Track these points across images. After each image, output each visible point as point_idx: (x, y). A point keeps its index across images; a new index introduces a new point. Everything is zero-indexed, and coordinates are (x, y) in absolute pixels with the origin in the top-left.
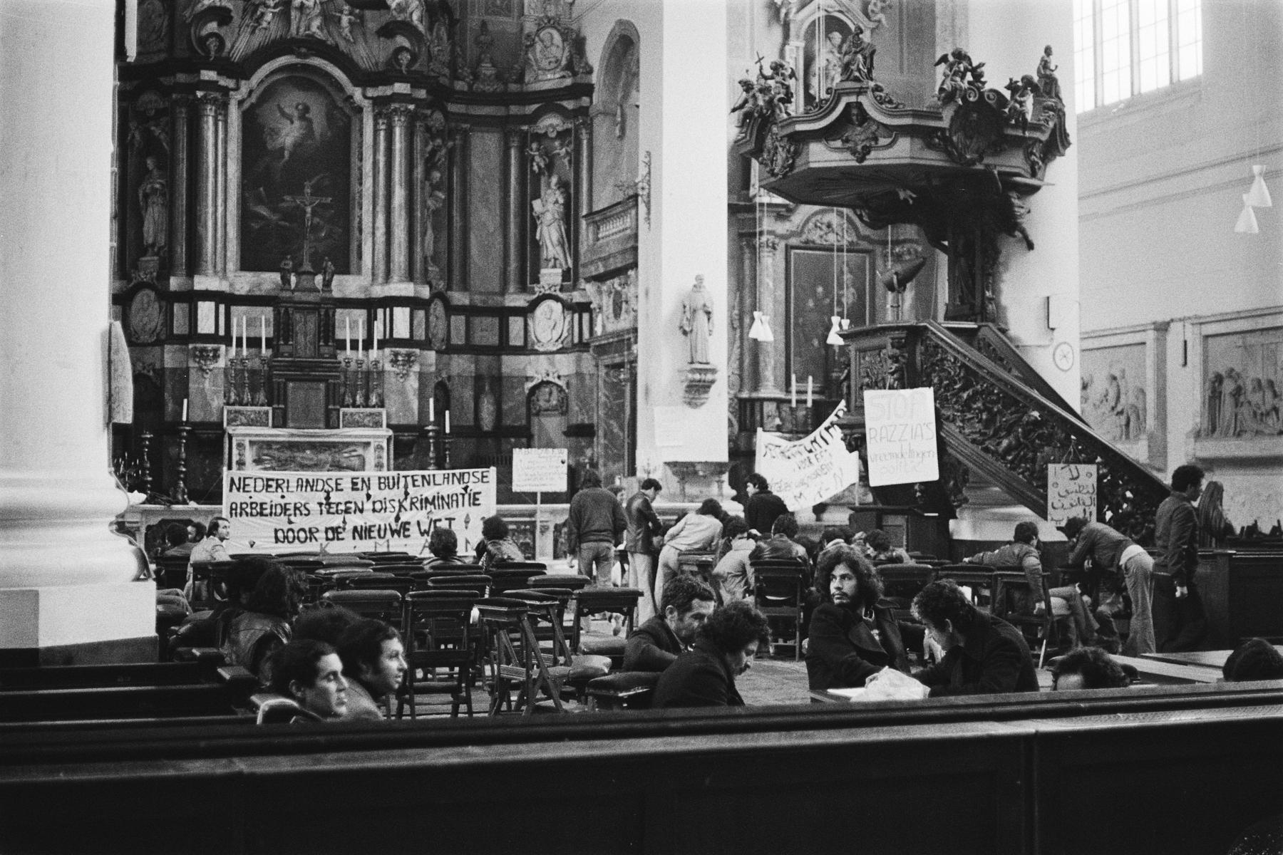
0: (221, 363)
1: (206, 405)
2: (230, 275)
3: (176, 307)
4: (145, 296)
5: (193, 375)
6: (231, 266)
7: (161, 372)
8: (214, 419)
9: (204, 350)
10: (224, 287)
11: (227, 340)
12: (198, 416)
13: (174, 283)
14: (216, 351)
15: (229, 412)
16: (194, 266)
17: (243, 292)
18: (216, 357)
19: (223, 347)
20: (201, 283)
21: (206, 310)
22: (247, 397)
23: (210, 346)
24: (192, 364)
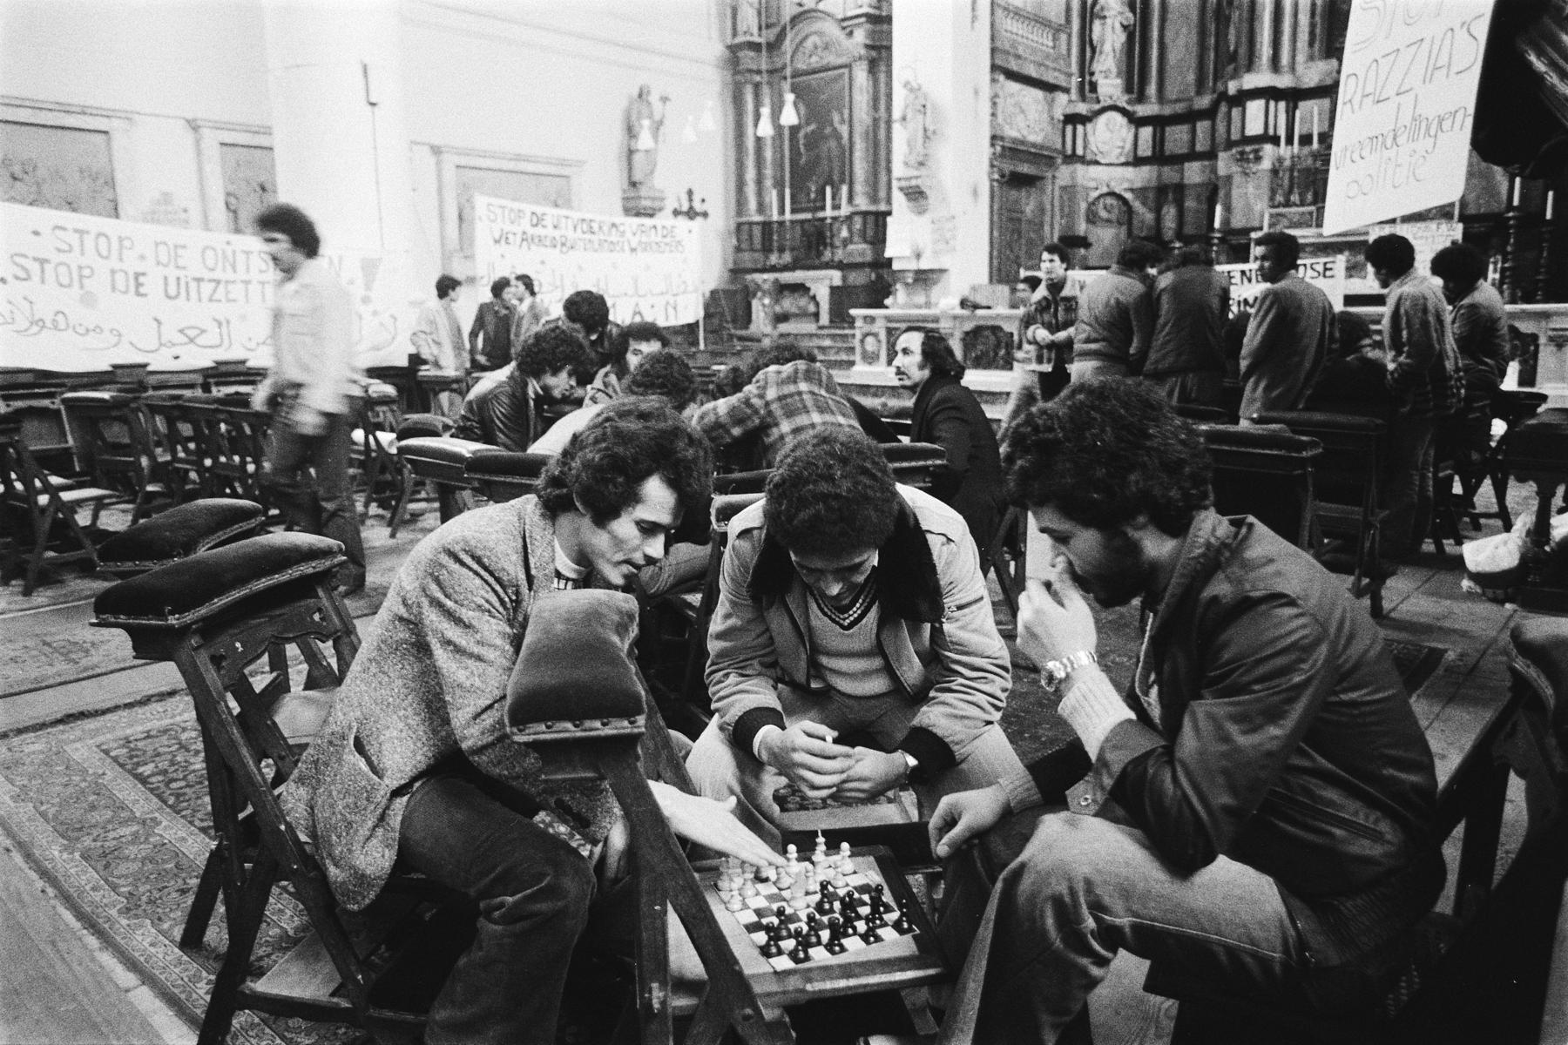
0: (1266, 164)
1: (1248, 208)
2: (1300, 68)
3: (1235, 112)
4: (1223, 108)
5: (1237, 179)
6: (1300, 58)
7: (1218, 178)
8: (1256, 224)
9: (1242, 153)
10: (1284, 81)
11: (1275, 140)
12: (1238, 222)
13: (1232, 87)
14: (1256, 151)
15: (1272, 216)
16: (1250, 66)
17: (1312, 84)
18: (1258, 159)
19: (1268, 149)
20: (1250, 81)
21: (1255, 108)
22: (1295, 198)
23: (1248, 149)
24: (1235, 169)
